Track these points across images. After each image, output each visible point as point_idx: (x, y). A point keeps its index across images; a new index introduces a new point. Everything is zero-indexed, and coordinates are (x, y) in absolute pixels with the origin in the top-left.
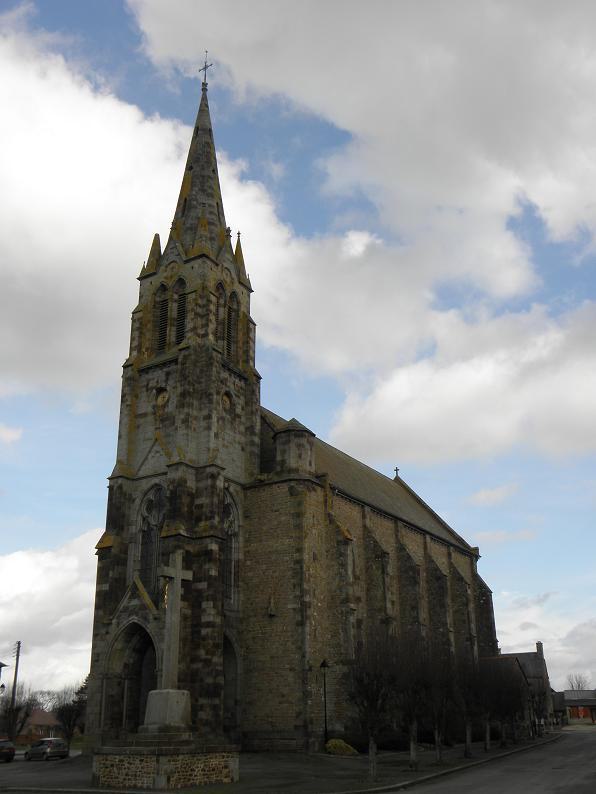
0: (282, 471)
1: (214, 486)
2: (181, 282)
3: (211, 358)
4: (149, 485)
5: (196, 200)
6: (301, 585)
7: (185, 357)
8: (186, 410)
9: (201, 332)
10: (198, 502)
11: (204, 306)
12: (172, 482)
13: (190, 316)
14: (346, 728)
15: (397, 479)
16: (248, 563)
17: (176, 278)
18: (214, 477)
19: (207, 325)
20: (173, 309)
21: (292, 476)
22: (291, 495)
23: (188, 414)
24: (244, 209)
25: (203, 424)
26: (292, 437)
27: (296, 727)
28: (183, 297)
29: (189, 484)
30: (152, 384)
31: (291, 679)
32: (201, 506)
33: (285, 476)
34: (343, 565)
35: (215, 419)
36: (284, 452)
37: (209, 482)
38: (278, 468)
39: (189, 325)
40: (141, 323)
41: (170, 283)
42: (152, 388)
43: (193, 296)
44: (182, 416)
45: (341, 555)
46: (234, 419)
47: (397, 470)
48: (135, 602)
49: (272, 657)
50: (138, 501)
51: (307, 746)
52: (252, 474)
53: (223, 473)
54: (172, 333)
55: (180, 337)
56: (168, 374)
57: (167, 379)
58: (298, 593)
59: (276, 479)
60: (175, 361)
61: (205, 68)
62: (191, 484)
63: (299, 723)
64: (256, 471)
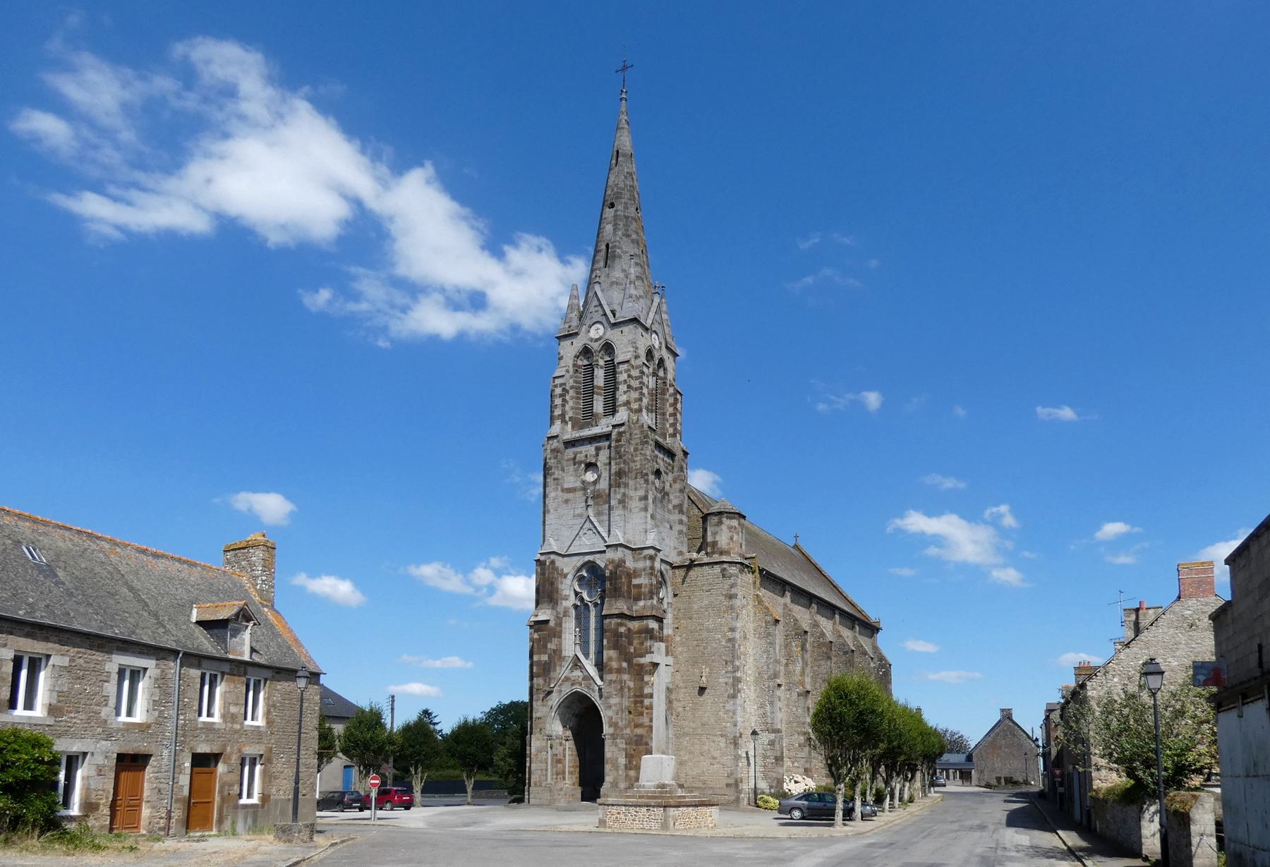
0: (713, 553)
1: (652, 568)
2: (608, 348)
3: (646, 436)
4: (581, 563)
5: (620, 248)
6: (732, 662)
7: (620, 434)
8: (622, 490)
9: (635, 406)
10: (635, 581)
11: (637, 378)
12: (612, 562)
13: (623, 388)
14: (771, 787)
15: (796, 547)
16: (678, 639)
17: (602, 342)
18: (652, 558)
19: (641, 400)
20: (600, 377)
21: (724, 558)
22: (724, 576)
23: (624, 495)
24: (1139, 862)
25: (642, 504)
26: (724, 520)
27: (728, 785)
28: (612, 369)
29: (628, 564)
30: (580, 457)
31: (722, 745)
32: (639, 586)
33: (716, 558)
34: (772, 644)
35: (650, 500)
36: (715, 534)
37: (648, 563)
38: (709, 550)
39: (622, 398)
40: (564, 389)
41: (596, 346)
42: (580, 463)
43: (625, 366)
44: (619, 496)
45: (769, 634)
46: (663, 497)
47: (796, 537)
48: (577, 673)
49: (703, 725)
50: (570, 577)
51: (738, 800)
52: (680, 553)
53: (661, 555)
54: (599, 405)
55: (612, 409)
56: (598, 449)
57: (597, 455)
58: (730, 669)
59: (706, 560)
60: (607, 436)
61: (625, 68)
62: (630, 564)
63: (731, 781)
64: (685, 549)
